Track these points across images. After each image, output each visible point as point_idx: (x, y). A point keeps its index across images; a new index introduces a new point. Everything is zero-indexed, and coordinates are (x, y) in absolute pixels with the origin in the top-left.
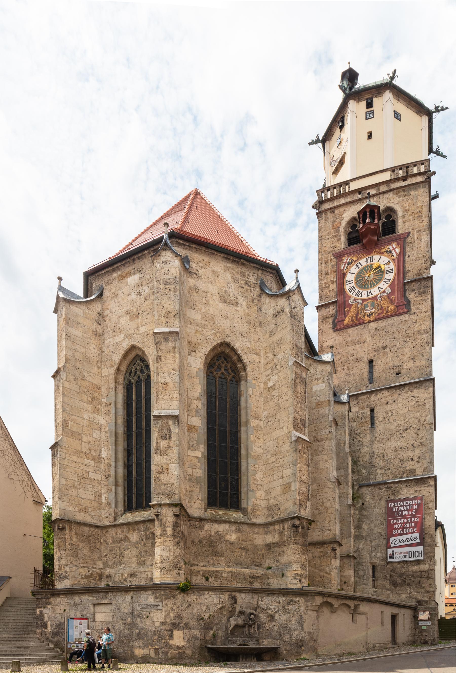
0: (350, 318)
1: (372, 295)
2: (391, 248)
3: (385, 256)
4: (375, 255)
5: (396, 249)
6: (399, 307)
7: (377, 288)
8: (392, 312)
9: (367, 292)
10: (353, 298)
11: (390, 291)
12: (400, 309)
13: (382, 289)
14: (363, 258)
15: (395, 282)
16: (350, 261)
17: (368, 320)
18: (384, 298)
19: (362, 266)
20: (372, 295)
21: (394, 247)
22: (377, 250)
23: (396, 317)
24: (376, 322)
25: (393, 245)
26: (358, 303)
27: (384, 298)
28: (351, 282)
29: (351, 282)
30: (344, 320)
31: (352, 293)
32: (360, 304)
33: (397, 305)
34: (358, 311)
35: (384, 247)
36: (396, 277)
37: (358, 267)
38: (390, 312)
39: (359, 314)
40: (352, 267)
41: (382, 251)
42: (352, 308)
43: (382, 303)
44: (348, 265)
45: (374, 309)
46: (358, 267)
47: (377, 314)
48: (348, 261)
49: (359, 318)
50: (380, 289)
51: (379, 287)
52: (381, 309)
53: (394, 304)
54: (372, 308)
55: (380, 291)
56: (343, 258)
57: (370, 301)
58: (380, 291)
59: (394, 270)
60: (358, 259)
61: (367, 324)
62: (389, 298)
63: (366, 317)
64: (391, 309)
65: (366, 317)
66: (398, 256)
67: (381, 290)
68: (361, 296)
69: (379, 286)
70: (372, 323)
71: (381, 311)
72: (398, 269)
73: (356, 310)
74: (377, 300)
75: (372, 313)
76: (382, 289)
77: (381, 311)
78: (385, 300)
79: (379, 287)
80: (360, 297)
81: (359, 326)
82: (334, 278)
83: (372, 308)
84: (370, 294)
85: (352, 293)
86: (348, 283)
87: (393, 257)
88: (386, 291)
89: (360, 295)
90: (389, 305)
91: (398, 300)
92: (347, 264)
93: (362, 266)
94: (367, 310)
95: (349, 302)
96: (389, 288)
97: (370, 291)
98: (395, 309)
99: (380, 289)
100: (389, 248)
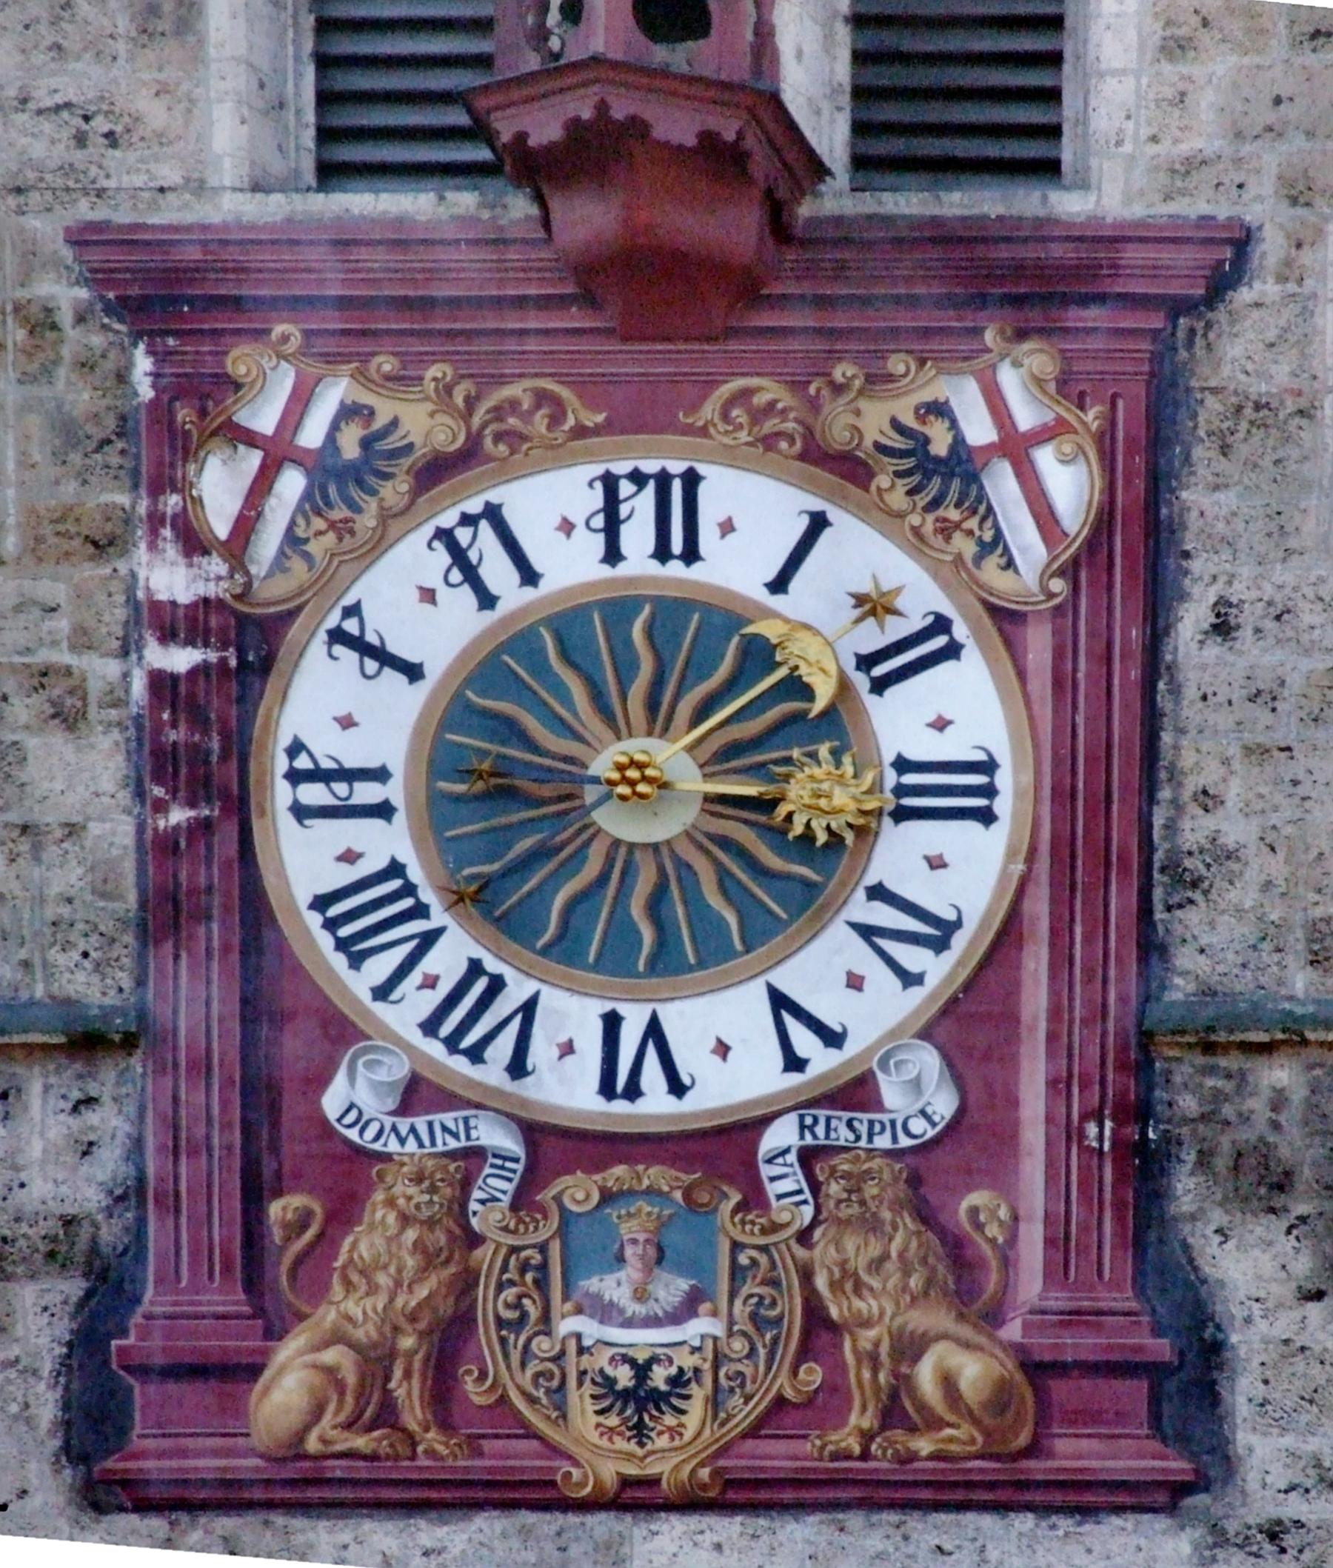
0: (331, 1356)
1: (677, 1087)
2: (980, 431)
3: (887, 520)
4: (731, 458)
5: (1045, 457)
6: (1060, 1389)
7: (752, 999)
8: (960, 1435)
9: (612, 1023)
10: (396, 1070)
11: (944, 1105)
12: (1084, 1417)
13: (832, 1038)
14: (556, 456)
15: (1012, 991)
16: (350, 447)
17: (609, 1471)
18: (855, 1183)
19: (529, 576)
20: (677, 1087)
21: (1026, 416)
22: (769, 390)
23: (1025, 1522)
24: (729, 1527)
25: (1009, 379)
26: (475, 1155)
27: (855, 1183)
28: (367, 793)
29: (367, 793)
30: (253, 1371)
31: (381, 966)
32: (504, 1188)
33: (1044, 1345)
34: (467, 1283)
35: (878, 380)
36: (1039, 907)
37: (471, 576)
38: (935, 1423)
39: (486, 1335)
40: (378, 546)
41: (837, 434)
42: (378, 1212)
43: (823, 1254)
44: (313, 502)
45: (700, 1327)
46: (471, 576)
47: (742, 1412)
48: (312, 435)
49: (474, 1391)
50: (804, 1041)
51: (780, 1002)
52: (805, 1353)
53: (993, 1317)
54: (672, 1288)
55: (794, 1063)
56: (240, 360)
57: (656, 1175)
58: (794, 1063)
59: (1004, 779)
60: (468, 456)
61: (601, 1523)
62: (926, 1217)
63: (582, 1404)
64: (948, 1382)
65: (582, 1404)
66: (1070, 571)
67: (821, 1060)
68: (518, 1067)
69: (786, 979)
70: (673, 1529)
71: (813, 1375)
72: (1063, 796)
73: (429, 1259)
74: (754, 1198)
75: (678, 1381)
76: (832, 1038)
77: (813, 1375)
78: (871, 1225)
79: (780, 1002)
80: (493, 1072)
81: (487, 1525)
82: (82, 640)
83: (672, 1288)
84: (652, 1073)
85: (381, 966)
86: (313, 794)
87: (991, 572)
88: (892, 1093)
89: (503, 1047)
90: (920, 1320)
91: (1056, 1271)
92: (291, 484)
93: (529, 576)
94: (605, 1312)
95: (332, 1102)
96: (927, 1060)
97: (654, 1031)
98: (1001, 1398)
99: (804, 1041)
100: (939, 409)
